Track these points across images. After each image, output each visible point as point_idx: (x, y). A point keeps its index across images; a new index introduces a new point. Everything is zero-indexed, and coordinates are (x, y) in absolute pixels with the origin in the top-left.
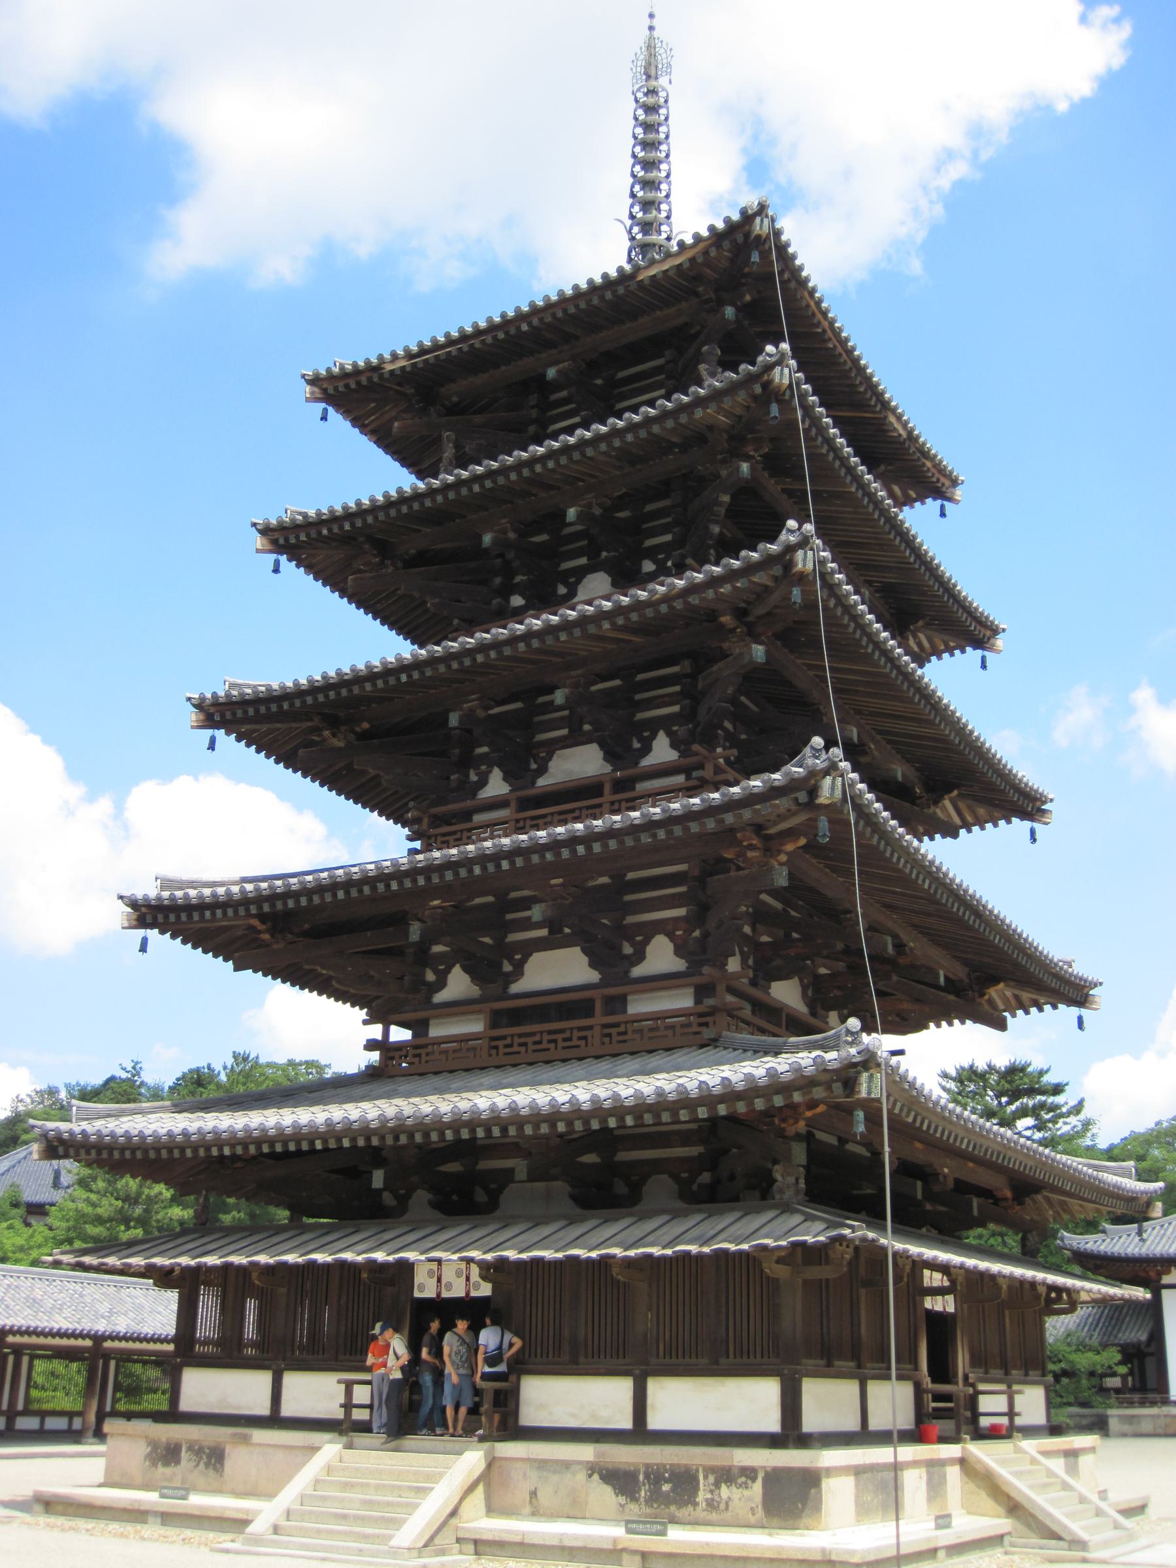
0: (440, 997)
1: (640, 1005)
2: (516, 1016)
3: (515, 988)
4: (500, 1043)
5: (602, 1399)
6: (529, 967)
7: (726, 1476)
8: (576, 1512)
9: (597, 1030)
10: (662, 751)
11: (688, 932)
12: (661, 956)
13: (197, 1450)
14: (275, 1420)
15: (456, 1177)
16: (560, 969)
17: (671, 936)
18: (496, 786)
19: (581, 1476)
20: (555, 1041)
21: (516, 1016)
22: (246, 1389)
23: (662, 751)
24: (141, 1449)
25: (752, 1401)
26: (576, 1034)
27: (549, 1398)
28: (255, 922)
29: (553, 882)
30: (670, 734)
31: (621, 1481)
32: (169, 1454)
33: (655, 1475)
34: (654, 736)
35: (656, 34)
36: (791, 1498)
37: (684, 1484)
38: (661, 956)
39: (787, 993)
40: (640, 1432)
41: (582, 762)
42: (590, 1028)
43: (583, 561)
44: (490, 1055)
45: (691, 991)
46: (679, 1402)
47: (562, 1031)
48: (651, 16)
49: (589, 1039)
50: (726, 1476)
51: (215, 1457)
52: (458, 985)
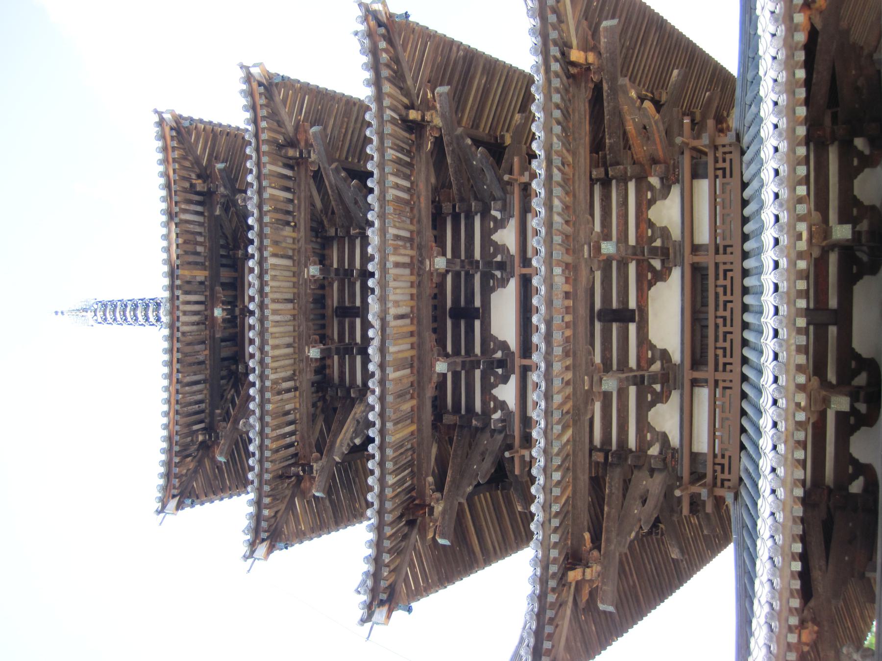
0: (674, 439)
1: (703, 236)
3: (676, 357)
4: (722, 360)
6: (660, 345)
9: (721, 258)
10: (507, 237)
11: (651, 187)
12: (667, 212)
17: (651, 203)
18: (507, 393)
20: (726, 303)
26: (721, 282)
28: (574, 576)
29: (586, 255)
30: (495, 230)
34: (495, 244)
35: (65, 309)
38: (667, 212)
42: (717, 265)
43: (358, 321)
44: (731, 371)
45: (695, 182)
47: (717, 295)
48: (56, 313)
49: (728, 267)
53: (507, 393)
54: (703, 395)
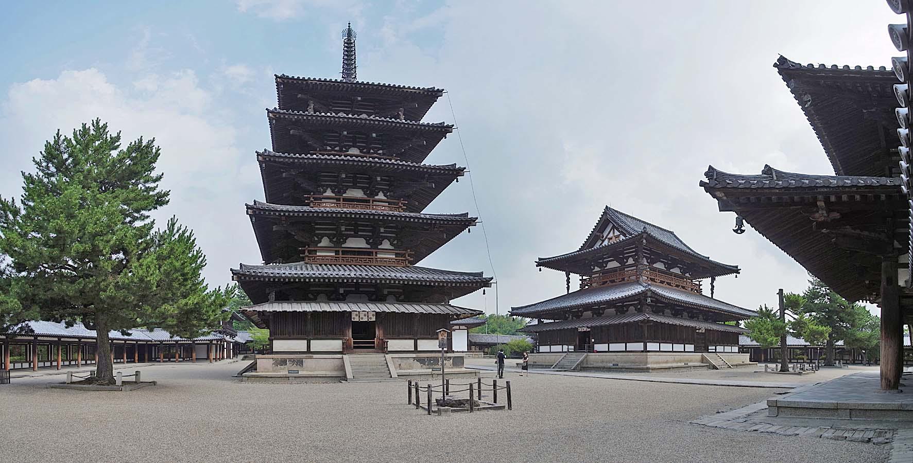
2: (344, 253)
5: (408, 344)
7: (446, 359)
8: (411, 367)
13: (293, 361)
18: (329, 193)
19: (412, 360)
22: (300, 345)
24: (271, 361)
27: (393, 345)
32: (283, 362)
33: (429, 359)
40: (416, 351)
41: (358, 194)
50: (446, 359)
51: (300, 362)
52: (325, 242)
53: (329, 193)
54: (333, 254)
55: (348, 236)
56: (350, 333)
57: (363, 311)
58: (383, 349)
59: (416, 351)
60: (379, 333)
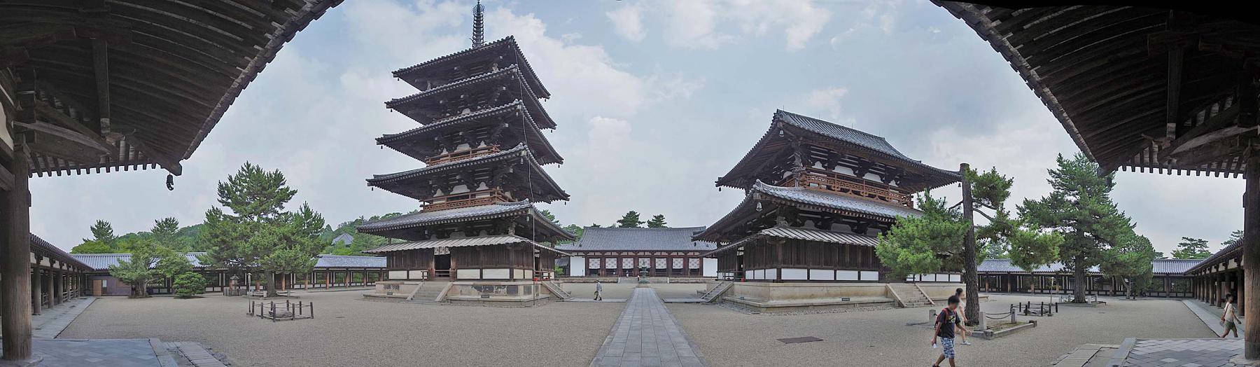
2: (452, 199)
5: (475, 273)
7: (500, 286)
8: (469, 294)
10: (483, 145)
12: (483, 187)
14: (408, 279)
15: (442, 230)
16: (461, 189)
21: (452, 199)
22: (402, 274)
23: (483, 145)
25: (504, 273)
27: (462, 273)
31: (478, 288)
33: (485, 286)
36: (513, 290)
37: (490, 288)
38: (483, 187)
39: (508, 194)
40: (481, 279)
41: (465, 147)
46: (489, 274)
50: (500, 286)
51: (397, 287)
52: (439, 193)
55: (455, 185)
56: (433, 265)
57: (440, 246)
58: (455, 278)
59: (481, 279)
60: (453, 264)
